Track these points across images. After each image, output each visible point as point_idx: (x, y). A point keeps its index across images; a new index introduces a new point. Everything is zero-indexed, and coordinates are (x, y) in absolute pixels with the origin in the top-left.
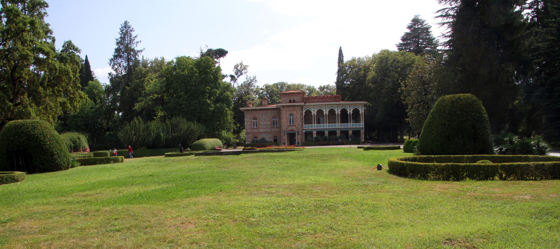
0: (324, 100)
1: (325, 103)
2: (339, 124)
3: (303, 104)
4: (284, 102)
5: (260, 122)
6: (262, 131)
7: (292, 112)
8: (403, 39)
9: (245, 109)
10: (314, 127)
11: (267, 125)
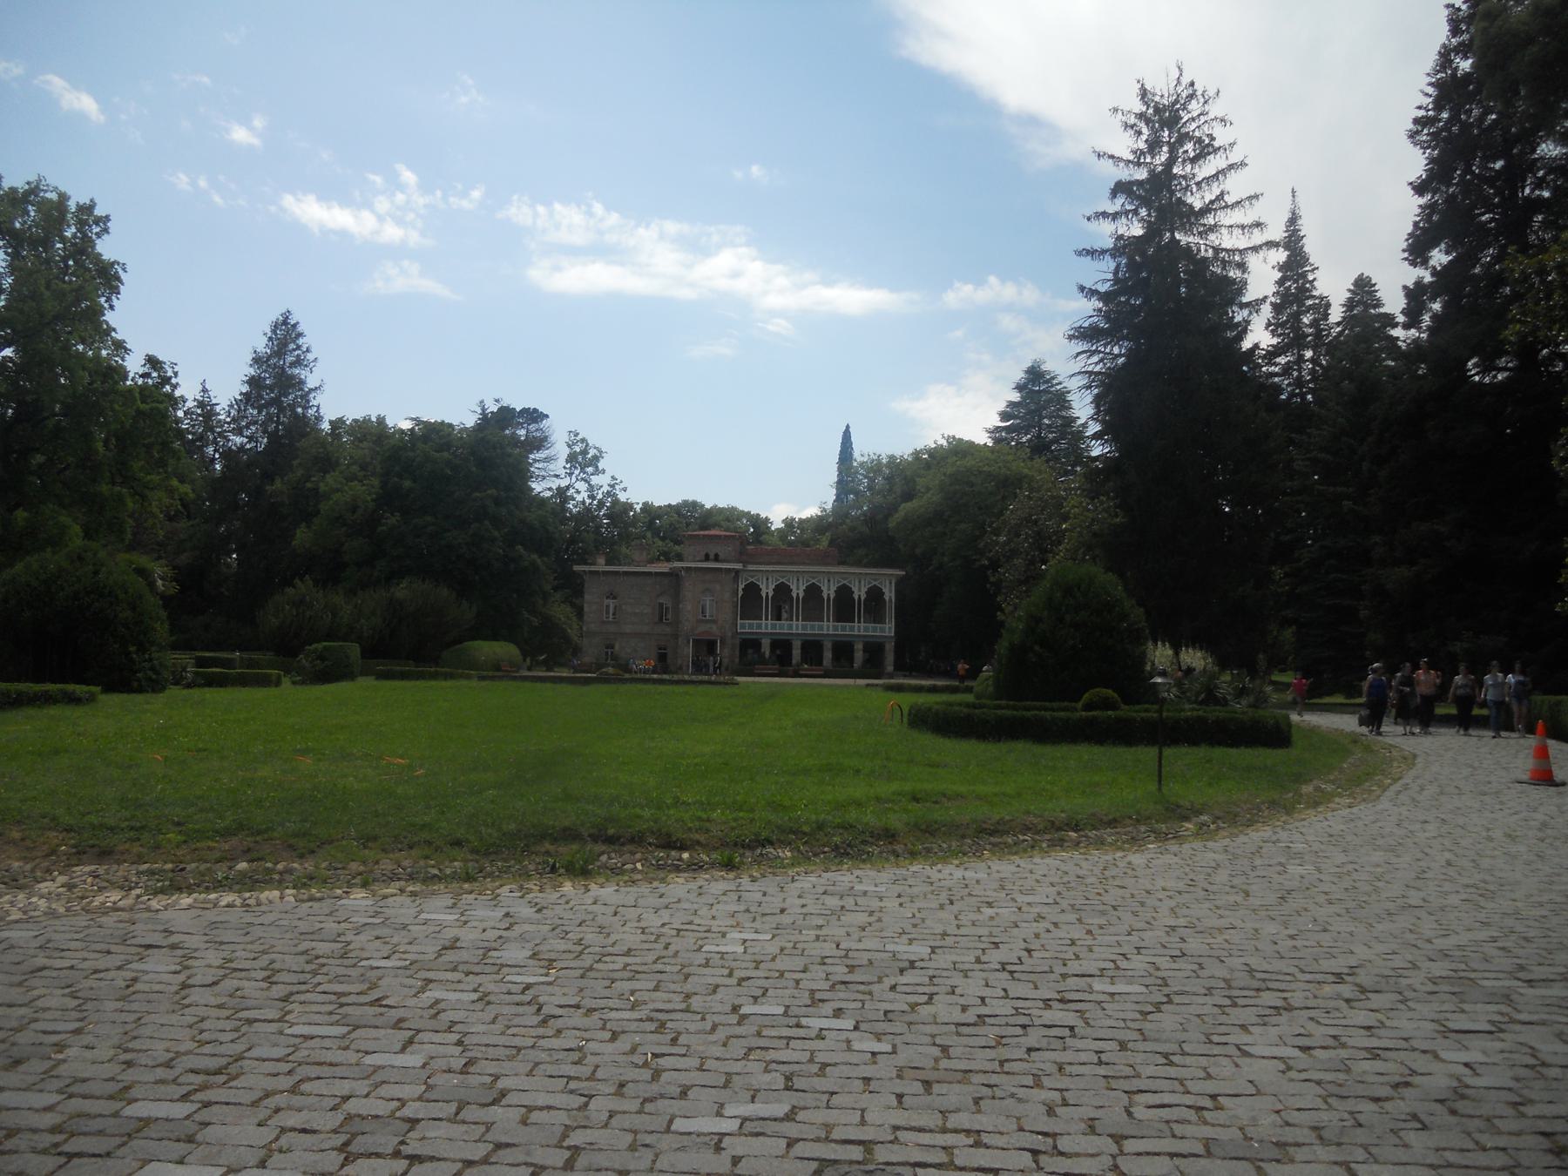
1: (795, 568)
3: (739, 566)
5: (624, 607)
6: (628, 631)
8: (1004, 416)
9: (586, 568)
10: (766, 626)
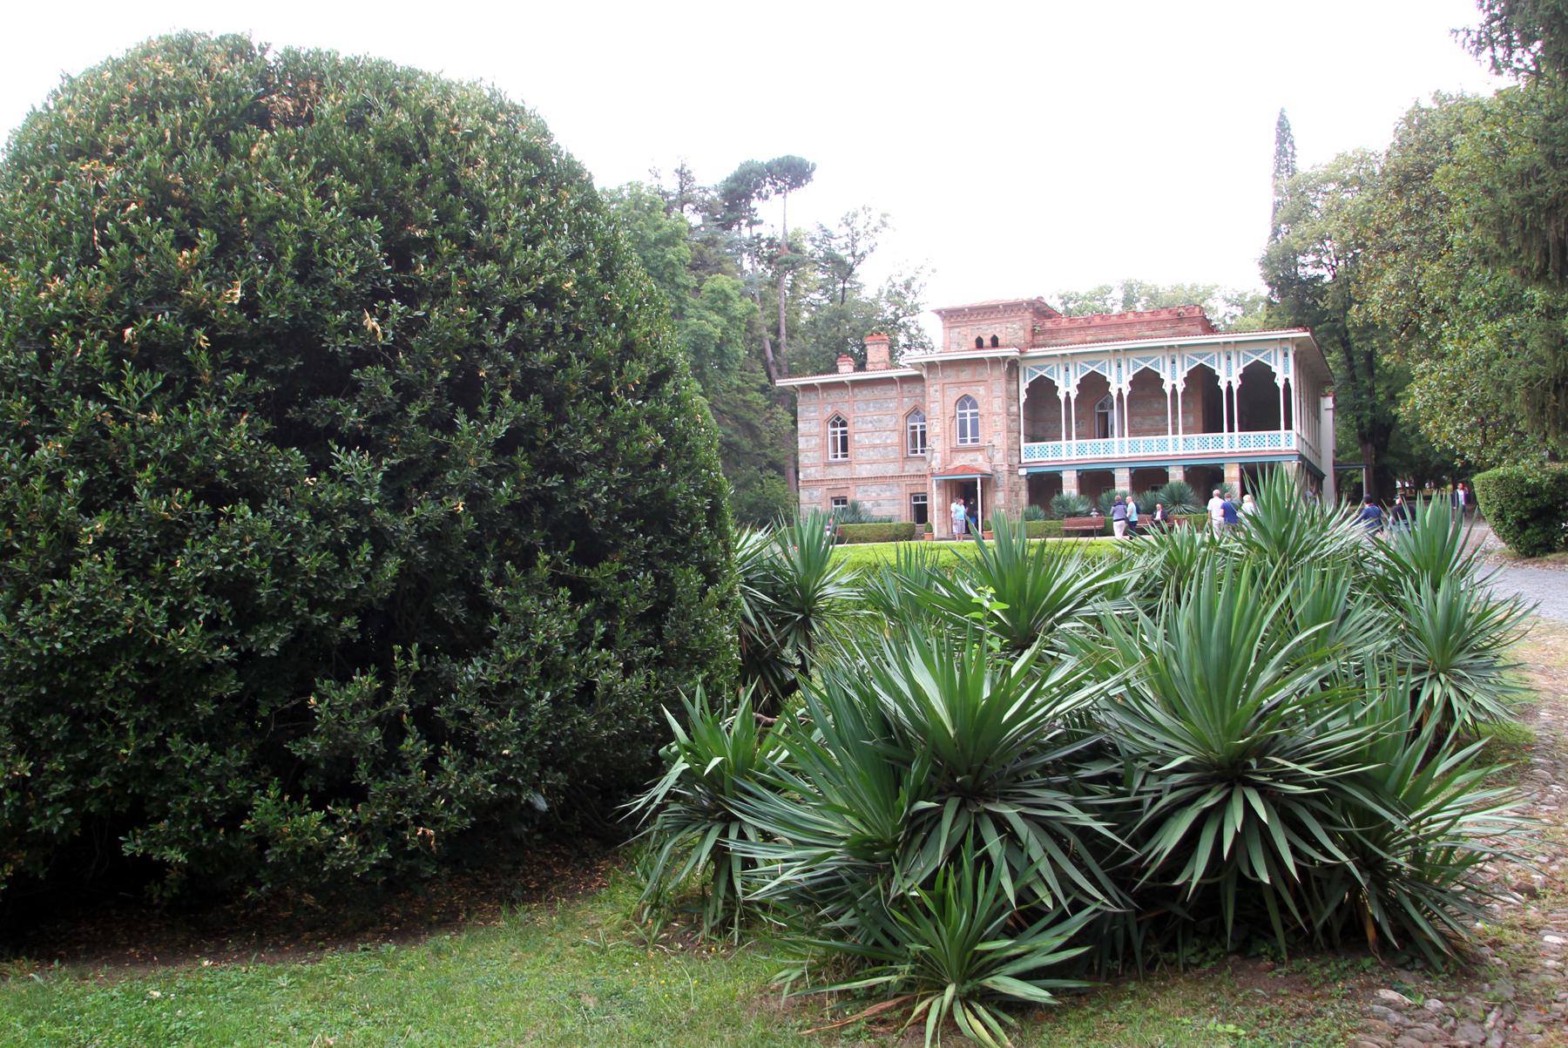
0: (1126, 331)
4: (954, 347)
6: (865, 475)
7: (969, 391)
11: (886, 446)
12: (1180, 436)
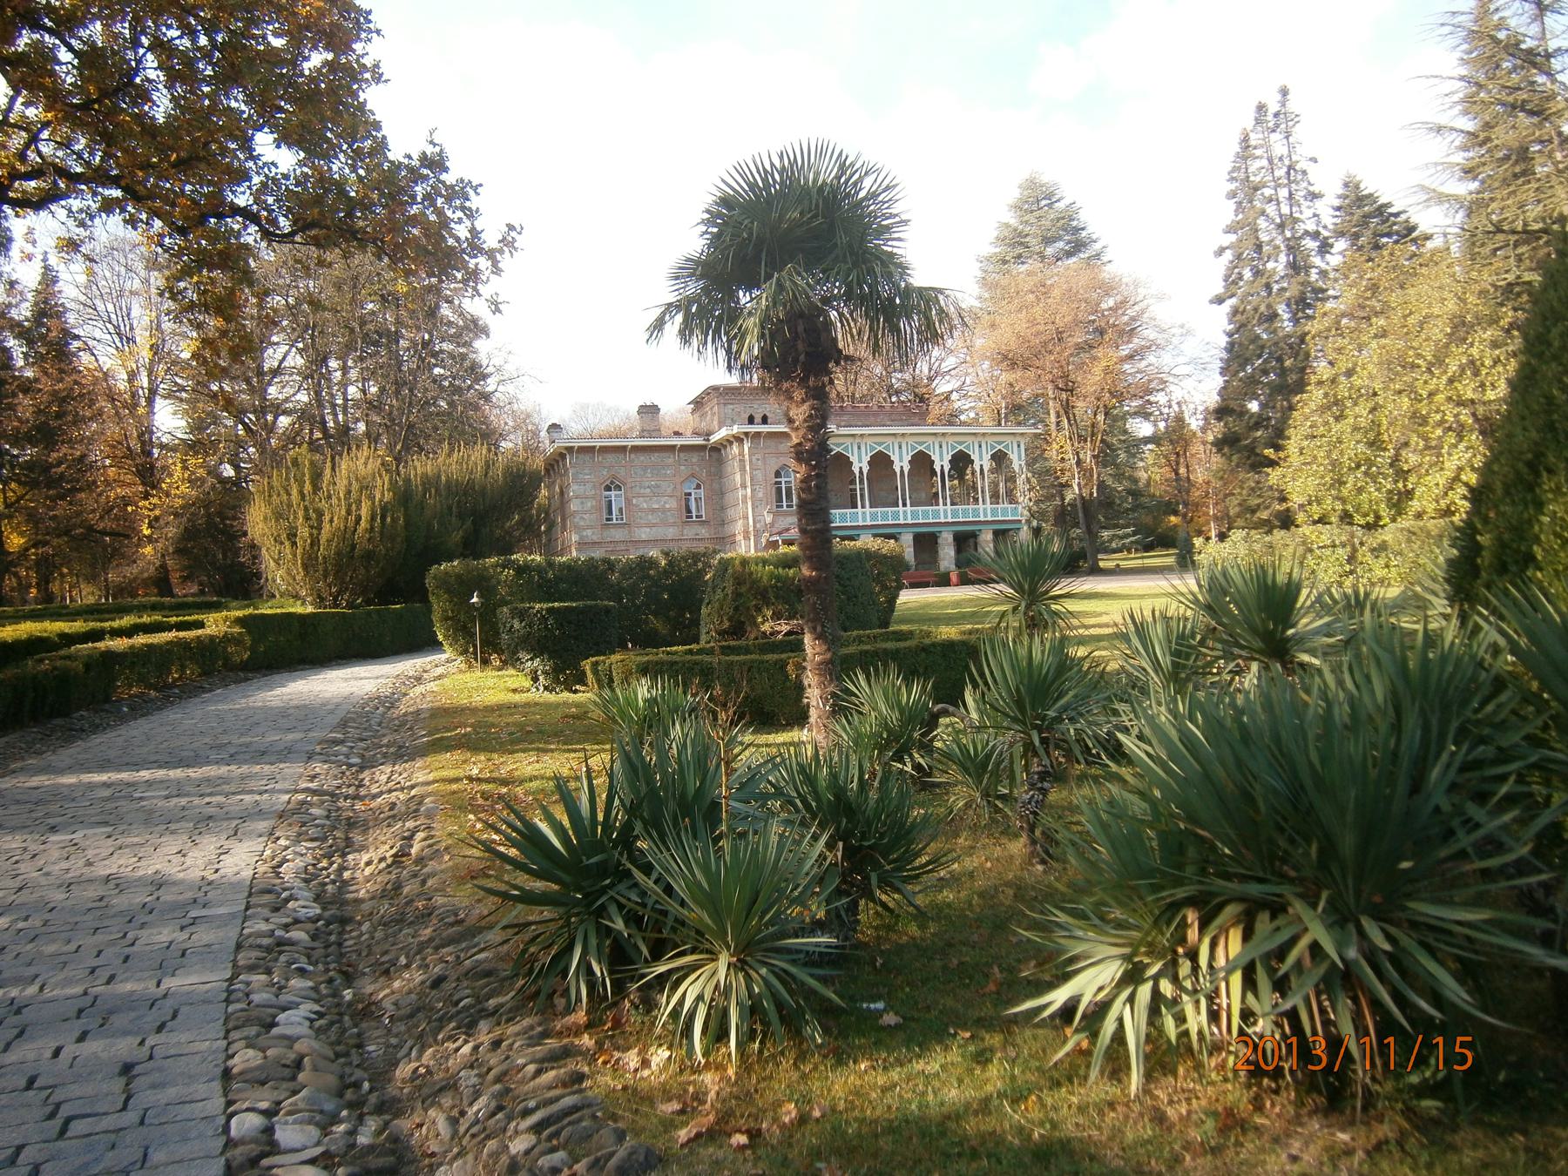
2: (988, 506)
6: (644, 537)
11: (664, 511)
12: (909, 508)
